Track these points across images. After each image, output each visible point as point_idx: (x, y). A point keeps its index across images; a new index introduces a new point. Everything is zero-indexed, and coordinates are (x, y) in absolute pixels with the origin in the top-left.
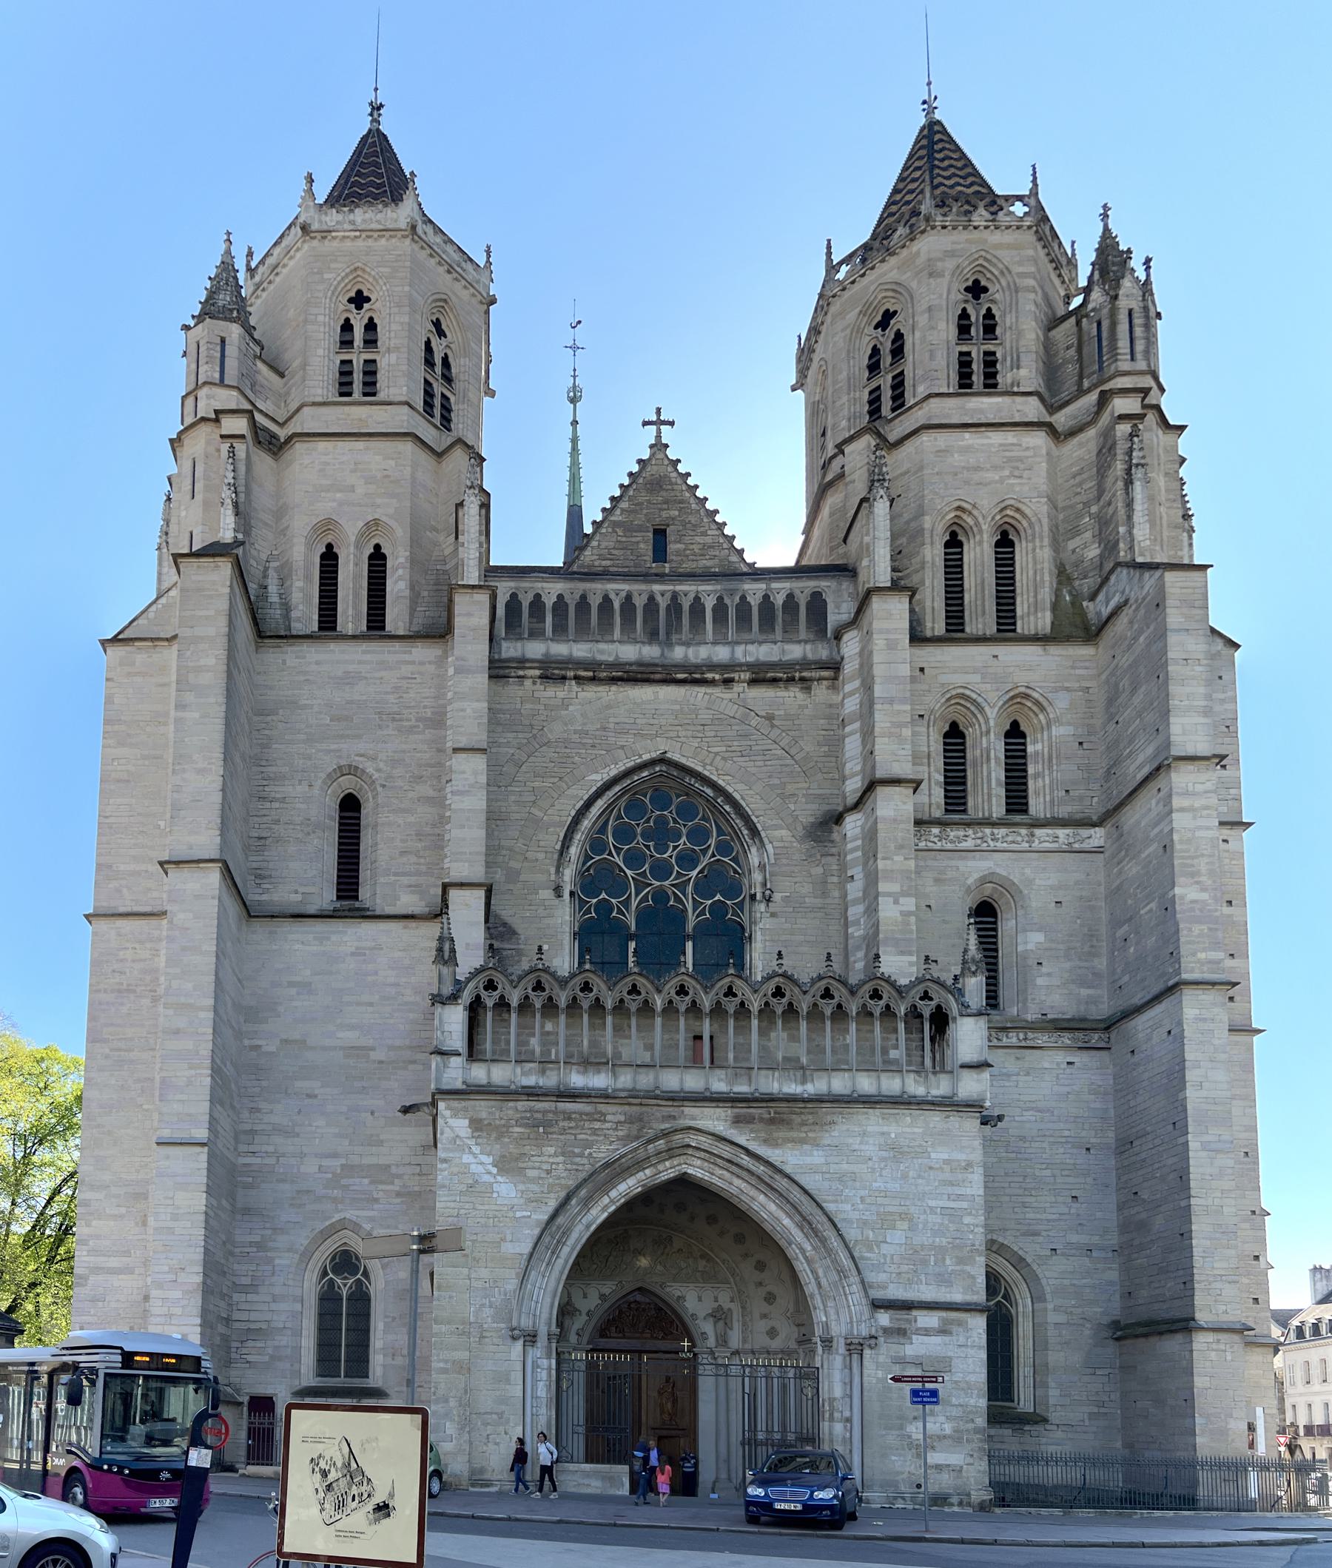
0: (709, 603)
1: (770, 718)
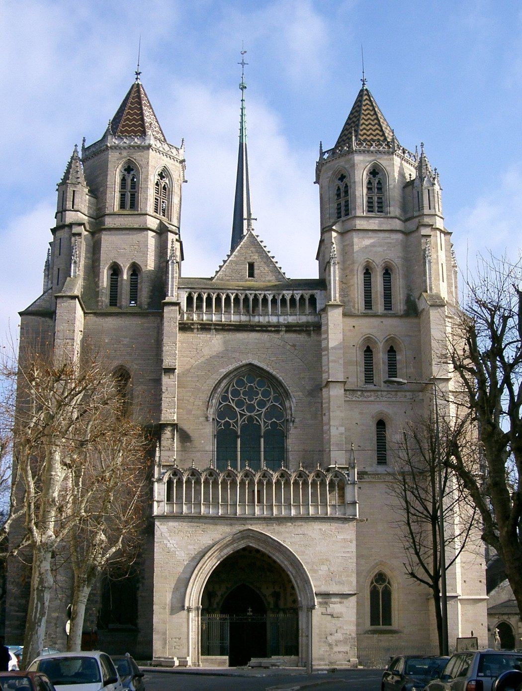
0: (270, 298)
1: (294, 346)
